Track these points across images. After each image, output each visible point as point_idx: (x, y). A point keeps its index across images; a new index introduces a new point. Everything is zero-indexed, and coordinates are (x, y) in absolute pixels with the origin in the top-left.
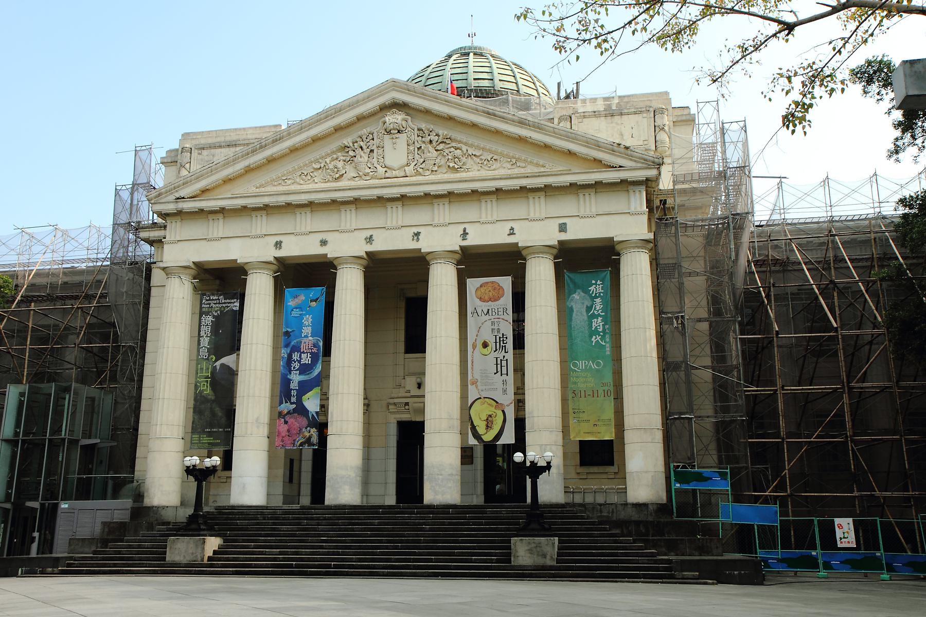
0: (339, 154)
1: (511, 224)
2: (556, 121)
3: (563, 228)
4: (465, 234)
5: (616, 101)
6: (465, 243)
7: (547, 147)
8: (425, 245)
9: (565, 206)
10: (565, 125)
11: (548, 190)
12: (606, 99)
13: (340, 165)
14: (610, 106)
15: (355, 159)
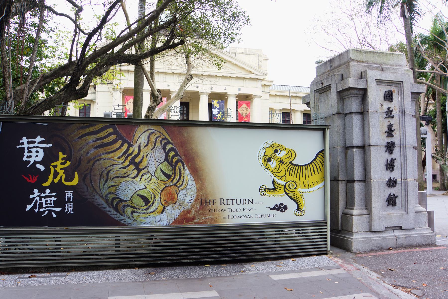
0: (173, 57)
1: (225, 87)
2: (231, 53)
3: (239, 89)
4: (212, 88)
5: (248, 50)
6: (212, 91)
7: (237, 65)
8: (201, 91)
9: (240, 83)
10: (233, 55)
11: (237, 78)
12: (245, 49)
13: (173, 61)
14: (246, 51)
15: (178, 60)
